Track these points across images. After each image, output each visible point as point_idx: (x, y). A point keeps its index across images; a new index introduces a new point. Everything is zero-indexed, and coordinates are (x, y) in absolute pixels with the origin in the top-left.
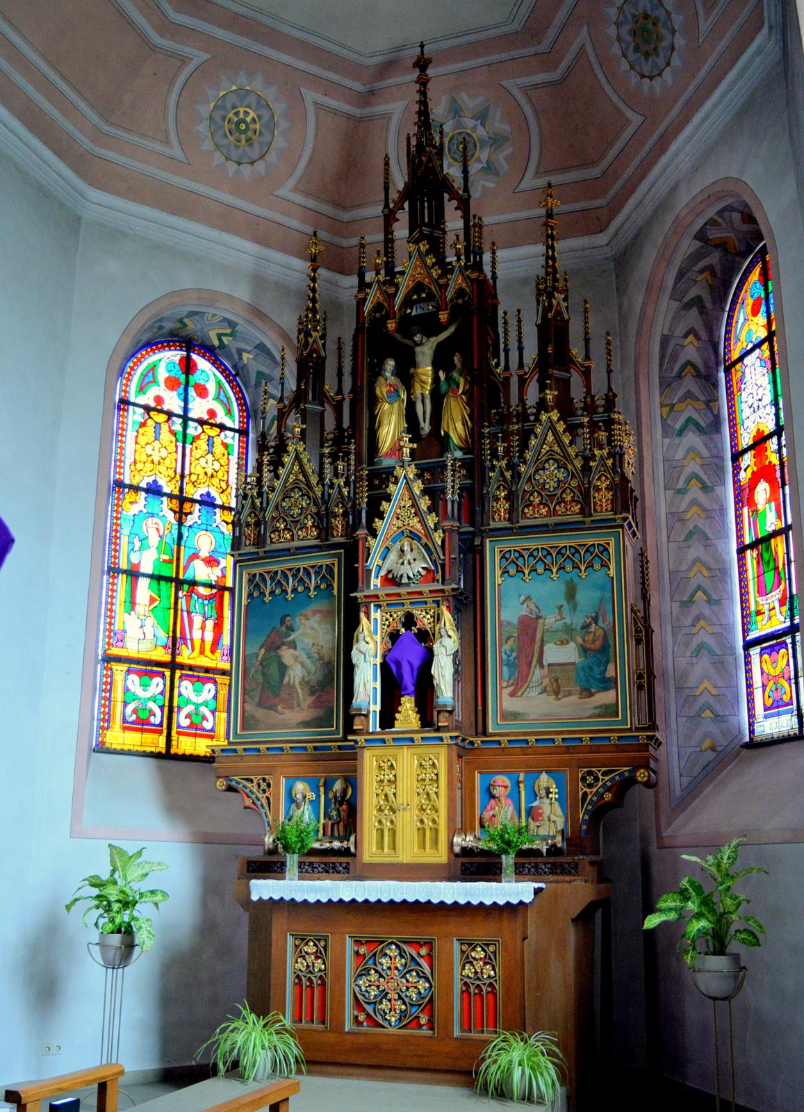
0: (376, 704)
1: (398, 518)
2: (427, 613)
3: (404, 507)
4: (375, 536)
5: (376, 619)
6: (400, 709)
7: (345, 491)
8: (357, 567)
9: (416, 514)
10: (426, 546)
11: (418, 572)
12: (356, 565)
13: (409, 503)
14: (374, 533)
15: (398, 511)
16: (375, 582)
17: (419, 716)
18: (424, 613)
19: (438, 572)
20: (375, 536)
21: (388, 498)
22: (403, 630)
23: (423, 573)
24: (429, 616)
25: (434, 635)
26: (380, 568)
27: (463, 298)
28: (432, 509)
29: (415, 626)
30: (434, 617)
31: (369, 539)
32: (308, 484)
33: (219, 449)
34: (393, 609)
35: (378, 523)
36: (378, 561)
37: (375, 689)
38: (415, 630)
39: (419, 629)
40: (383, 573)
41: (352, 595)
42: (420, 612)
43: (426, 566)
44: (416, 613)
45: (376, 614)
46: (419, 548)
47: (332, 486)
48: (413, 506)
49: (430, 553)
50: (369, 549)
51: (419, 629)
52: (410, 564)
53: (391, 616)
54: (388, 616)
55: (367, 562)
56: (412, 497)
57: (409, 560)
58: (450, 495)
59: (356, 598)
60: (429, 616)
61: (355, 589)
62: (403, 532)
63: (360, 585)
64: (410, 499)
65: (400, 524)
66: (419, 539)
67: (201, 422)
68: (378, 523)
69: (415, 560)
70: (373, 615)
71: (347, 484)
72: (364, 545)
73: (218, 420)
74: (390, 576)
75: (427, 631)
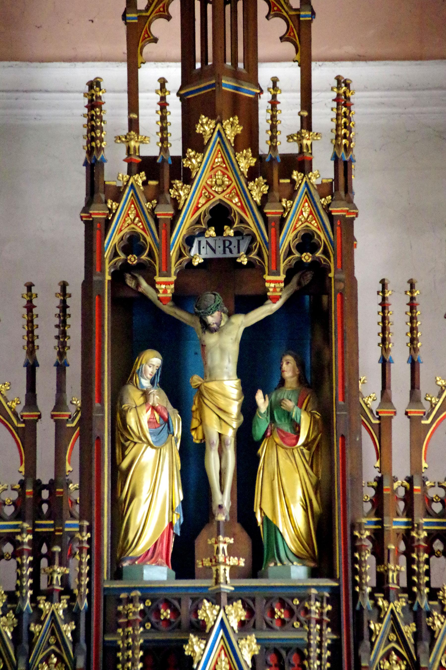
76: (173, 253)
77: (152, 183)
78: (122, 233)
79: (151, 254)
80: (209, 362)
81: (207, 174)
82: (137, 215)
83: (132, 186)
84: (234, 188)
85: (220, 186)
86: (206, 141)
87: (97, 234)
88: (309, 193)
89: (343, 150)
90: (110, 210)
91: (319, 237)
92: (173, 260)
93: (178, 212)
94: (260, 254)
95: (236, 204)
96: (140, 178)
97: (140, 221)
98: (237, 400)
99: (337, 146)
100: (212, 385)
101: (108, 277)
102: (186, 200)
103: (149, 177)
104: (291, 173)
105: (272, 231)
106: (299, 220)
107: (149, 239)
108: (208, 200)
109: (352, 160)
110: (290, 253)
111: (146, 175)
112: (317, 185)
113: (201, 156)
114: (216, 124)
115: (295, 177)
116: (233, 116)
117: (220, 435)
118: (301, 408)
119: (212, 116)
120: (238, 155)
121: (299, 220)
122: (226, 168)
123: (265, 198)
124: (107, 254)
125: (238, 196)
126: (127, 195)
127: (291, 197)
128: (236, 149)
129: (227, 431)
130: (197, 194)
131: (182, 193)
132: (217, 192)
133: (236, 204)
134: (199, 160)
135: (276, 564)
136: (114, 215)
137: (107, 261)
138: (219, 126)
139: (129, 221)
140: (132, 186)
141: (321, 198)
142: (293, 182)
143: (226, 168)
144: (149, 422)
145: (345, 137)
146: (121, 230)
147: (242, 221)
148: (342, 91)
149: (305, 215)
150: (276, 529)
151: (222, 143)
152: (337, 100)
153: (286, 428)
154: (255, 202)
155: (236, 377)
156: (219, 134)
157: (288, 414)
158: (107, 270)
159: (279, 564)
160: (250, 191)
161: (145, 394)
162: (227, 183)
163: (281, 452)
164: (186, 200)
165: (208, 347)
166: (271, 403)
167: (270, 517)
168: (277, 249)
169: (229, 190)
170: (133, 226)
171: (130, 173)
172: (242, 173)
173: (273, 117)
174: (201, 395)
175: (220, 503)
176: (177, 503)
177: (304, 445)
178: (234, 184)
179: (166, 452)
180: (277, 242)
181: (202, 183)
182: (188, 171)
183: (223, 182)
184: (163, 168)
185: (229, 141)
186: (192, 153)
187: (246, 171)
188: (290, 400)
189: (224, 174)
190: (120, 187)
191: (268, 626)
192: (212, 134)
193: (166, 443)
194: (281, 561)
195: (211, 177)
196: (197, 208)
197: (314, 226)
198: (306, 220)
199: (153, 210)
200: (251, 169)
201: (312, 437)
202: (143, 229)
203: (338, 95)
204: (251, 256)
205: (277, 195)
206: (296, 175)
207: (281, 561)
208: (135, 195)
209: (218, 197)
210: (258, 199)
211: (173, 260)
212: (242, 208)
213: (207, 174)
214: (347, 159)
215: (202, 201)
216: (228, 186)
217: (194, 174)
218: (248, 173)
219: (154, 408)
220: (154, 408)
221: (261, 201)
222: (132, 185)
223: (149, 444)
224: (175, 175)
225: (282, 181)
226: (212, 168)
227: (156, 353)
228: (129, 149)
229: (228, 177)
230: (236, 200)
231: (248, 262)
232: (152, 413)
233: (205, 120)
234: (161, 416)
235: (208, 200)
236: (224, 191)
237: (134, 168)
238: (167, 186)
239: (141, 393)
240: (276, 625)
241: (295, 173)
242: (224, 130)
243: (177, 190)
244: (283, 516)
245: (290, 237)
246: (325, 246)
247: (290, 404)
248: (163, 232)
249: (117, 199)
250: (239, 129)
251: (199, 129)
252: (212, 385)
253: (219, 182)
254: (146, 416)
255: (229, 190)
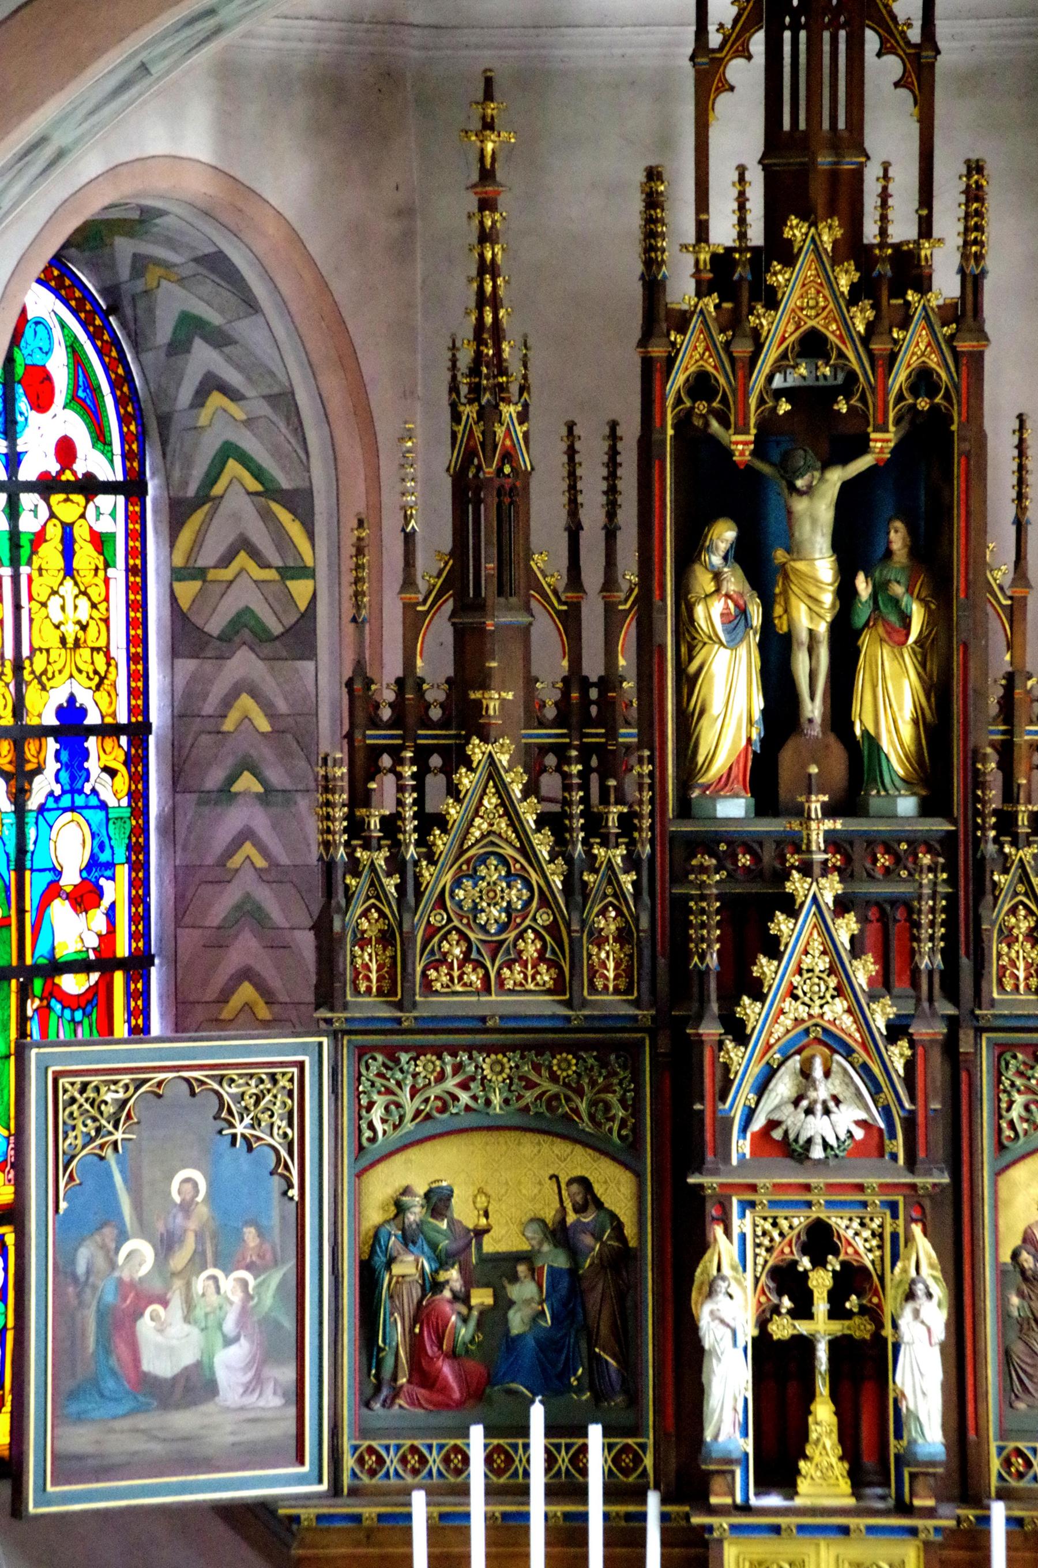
0: (746, 1435)
1: (796, 998)
2: (863, 1225)
3: (809, 971)
4: (742, 1039)
5: (743, 1237)
6: (809, 1450)
7: (627, 880)
8: (702, 1112)
9: (839, 991)
10: (865, 1070)
11: (849, 1132)
12: (698, 1107)
13: (823, 963)
14: (740, 1034)
15: (796, 980)
16: (741, 1147)
17: (846, 1466)
18: (856, 1224)
19: (893, 1136)
20: (742, 1039)
21: (773, 949)
22: (805, 1263)
23: (859, 1134)
24: (867, 1234)
25: (882, 1278)
26: (750, 1114)
27: (931, 396)
28: (883, 984)
29: (836, 1253)
30: (881, 1236)
31: (729, 1045)
32: (526, 850)
33: (85, 556)
34: (780, 1213)
35: (749, 1009)
36: (742, 1096)
37: (746, 1400)
38: (834, 1263)
39: (843, 1264)
40: (758, 1123)
41: (691, 1180)
42: (846, 1222)
43: (863, 1115)
44: (838, 1222)
45: (742, 1224)
46: (845, 1070)
47: (591, 863)
48: (831, 971)
49: (876, 1090)
50: (726, 1068)
51: (843, 1264)
52: (827, 1112)
53: (775, 1224)
54: (768, 1226)
55: (723, 1098)
56: (830, 948)
57: (824, 1102)
58: (926, 959)
59: (701, 1186)
60: (867, 1234)
61: (699, 1167)
62: (807, 1031)
63: (709, 1157)
64: (824, 953)
65: (803, 1012)
66: (848, 1052)
67: (46, 486)
68: (749, 1009)
69: (837, 1101)
70: (736, 1221)
71: (632, 862)
72: (715, 1058)
73: (80, 467)
74: (777, 1134)
75: (864, 1269)
76: (753, 401)
77: (727, 305)
78: (688, 373)
79: (724, 400)
80: (797, 534)
81: (797, 292)
82: (707, 349)
83: (701, 312)
84: (831, 311)
85: (812, 308)
86: (796, 250)
87: (657, 377)
88: (927, 318)
89: (972, 262)
90: (673, 344)
91: (939, 375)
92: (753, 408)
93: (759, 347)
94: (863, 399)
95: (833, 332)
96: (710, 302)
97: (711, 356)
98: (831, 584)
99: (965, 257)
100: (800, 565)
101: (670, 432)
102: (769, 331)
103: (722, 299)
104: (906, 293)
105: (880, 370)
106: (913, 354)
107: (722, 381)
108: (798, 327)
109: (983, 273)
110: (900, 398)
111: (719, 297)
112: (939, 307)
113: (789, 270)
114: (809, 228)
115: (910, 298)
116: (831, 217)
117: (811, 631)
118: (912, 594)
119: (803, 218)
120: (837, 269)
121: (913, 354)
122: (821, 284)
123: (870, 326)
124: (670, 401)
125: (836, 321)
126: (695, 321)
127: (904, 325)
128: (836, 261)
129: (817, 625)
130: (785, 319)
131: (764, 322)
132: (809, 317)
133: (833, 332)
134: (787, 276)
135: (878, 792)
136: (678, 351)
137: (669, 410)
138: (813, 230)
139: (698, 357)
140: (701, 312)
141: (943, 326)
142: (908, 304)
143: (821, 284)
144: (722, 615)
145: (975, 242)
146: (687, 369)
147: (841, 355)
148: (972, 181)
149: (922, 346)
150: (879, 748)
151: (817, 251)
152: (967, 191)
153: (893, 619)
154: (859, 333)
155: (830, 552)
156: (813, 240)
157: (895, 602)
158: (669, 422)
159: (883, 793)
160: (851, 318)
161: (717, 576)
162: (822, 304)
163: (886, 650)
164: (769, 331)
165: (796, 515)
166: (874, 586)
167: (872, 732)
168: (886, 392)
169: (825, 314)
170: (701, 363)
171: (699, 294)
172: (842, 293)
173: (884, 218)
174: (786, 577)
175: (809, 715)
176: (757, 715)
177: (915, 642)
178: (831, 306)
179: (742, 650)
180: (885, 383)
181: (791, 305)
182: (772, 290)
183: (817, 303)
184: (740, 287)
185: (825, 250)
186: (779, 267)
187: (845, 290)
188: (898, 582)
189: (818, 292)
190: (686, 311)
191: (869, 875)
192: (804, 241)
193: (741, 641)
194: (886, 790)
195: (802, 297)
196: (783, 339)
197: (933, 361)
198: (923, 354)
199: (727, 344)
200: (853, 286)
201: (926, 633)
202: (715, 367)
203: (968, 186)
204: (852, 402)
205: (886, 323)
206: (911, 296)
207: (886, 790)
208: (705, 322)
209: (811, 323)
210: (861, 328)
211: (753, 408)
212: (841, 337)
213: (797, 292)
214: (977, 272)
215: (791, 328)
216: (824, 308)
217: (780, 296)
218: (850, 292)
219: (728, 596)
220: (728, 596)
221: (866, 330)
222: (701, 311)
223: (721, 644)
224: (755, 297)
225: (893, 302)
226: (804, 285)
227: (731, 524)
228: (697, 262)
229: (824, 297)
230: (834, 327)
231: (849, 409)
232: (726, 603)
233: (795, 222)
234: (736, 605)
235: (798, 327)
236: (818, 315)
237: (704, 289)
238: (745, 310)
239: (711, 576)
240: (879, 875)
241: (910, 292)
242: (820, 235)
243: (758, 317)
244: (889, 732)
245: (902, 377)
246: (947, 387)
247: (898, 590)
248: (740, 374)
249: (682, 330)
250: (839, 233)
251: (787, 234)
252: (800, 565)
253: (812, 303)
254: (717, 606)
255: (825, 314)
